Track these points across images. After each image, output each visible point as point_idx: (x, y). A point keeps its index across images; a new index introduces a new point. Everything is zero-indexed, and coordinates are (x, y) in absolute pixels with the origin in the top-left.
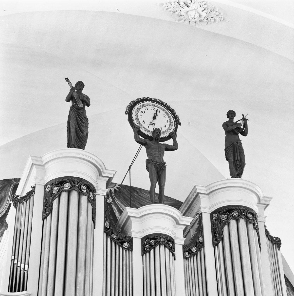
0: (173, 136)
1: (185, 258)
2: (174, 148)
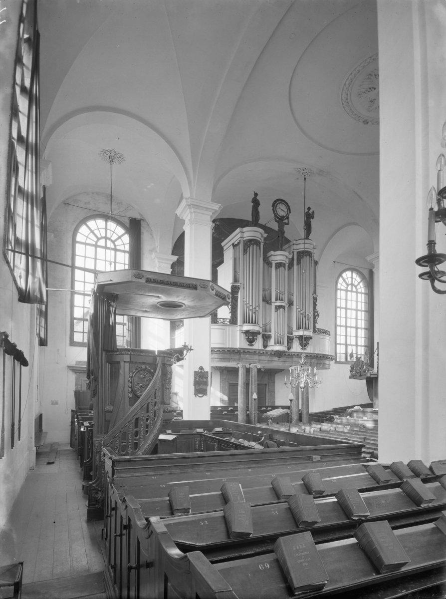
0: (288, 218)
1: (288, 270)
2: (288, 224)
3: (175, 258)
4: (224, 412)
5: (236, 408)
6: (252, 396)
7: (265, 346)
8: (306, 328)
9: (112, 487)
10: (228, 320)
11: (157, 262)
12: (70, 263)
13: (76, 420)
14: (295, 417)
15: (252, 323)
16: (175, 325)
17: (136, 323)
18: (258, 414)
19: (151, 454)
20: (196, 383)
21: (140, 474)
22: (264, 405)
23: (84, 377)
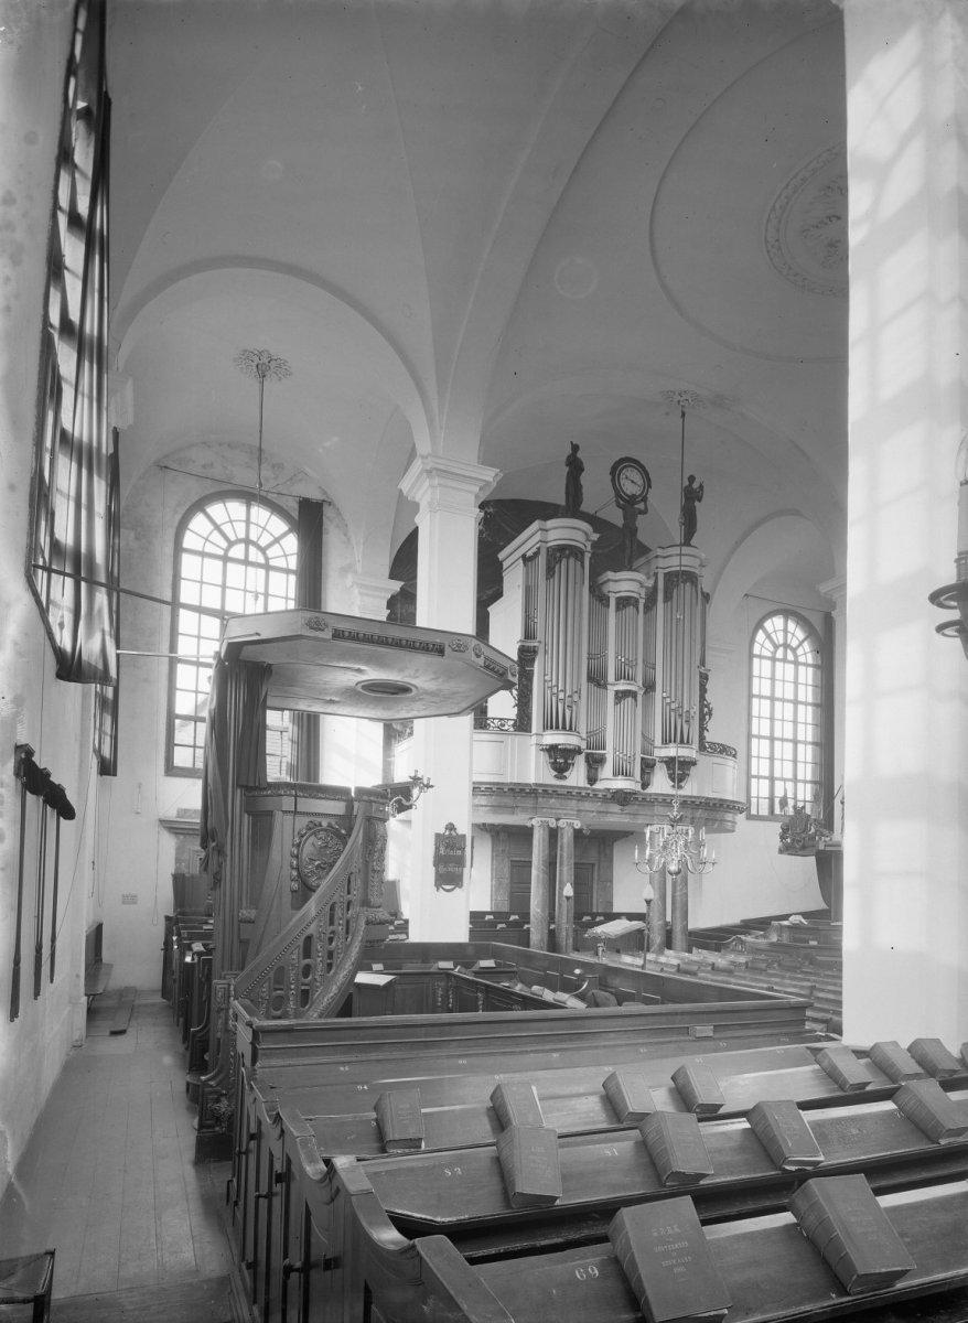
0: (644, 499)
1: (645, 613)
2: (644, 512)
3: (396, 586)
4: (500, 926)
5: (525, 917)
6: (561, 889)
7: (592, 780)
8: (682, 742)
9: (252, 1088)
10: (512, 722)
11: (356, 593)
12: (168, 596)
13: (175, 938)
14: (657, 938)
15: (564, 728)
16: (393, 733)
17: (309, 729)
18: (575, 931)
19: (338, 1016)
20: (439, 860)
21: (314, 1060)
22: (589, 910)
23: (195, 845)
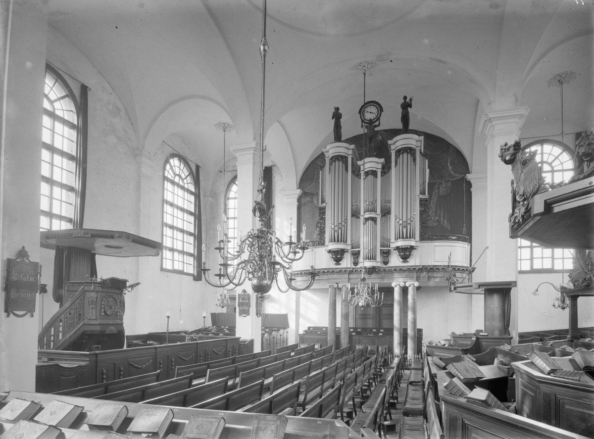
1: (382, 176)
7: (356, 264)
